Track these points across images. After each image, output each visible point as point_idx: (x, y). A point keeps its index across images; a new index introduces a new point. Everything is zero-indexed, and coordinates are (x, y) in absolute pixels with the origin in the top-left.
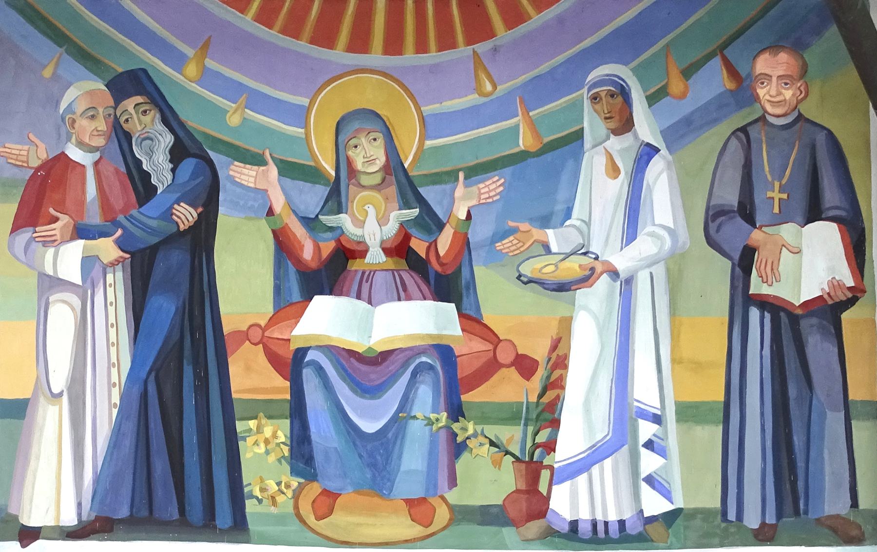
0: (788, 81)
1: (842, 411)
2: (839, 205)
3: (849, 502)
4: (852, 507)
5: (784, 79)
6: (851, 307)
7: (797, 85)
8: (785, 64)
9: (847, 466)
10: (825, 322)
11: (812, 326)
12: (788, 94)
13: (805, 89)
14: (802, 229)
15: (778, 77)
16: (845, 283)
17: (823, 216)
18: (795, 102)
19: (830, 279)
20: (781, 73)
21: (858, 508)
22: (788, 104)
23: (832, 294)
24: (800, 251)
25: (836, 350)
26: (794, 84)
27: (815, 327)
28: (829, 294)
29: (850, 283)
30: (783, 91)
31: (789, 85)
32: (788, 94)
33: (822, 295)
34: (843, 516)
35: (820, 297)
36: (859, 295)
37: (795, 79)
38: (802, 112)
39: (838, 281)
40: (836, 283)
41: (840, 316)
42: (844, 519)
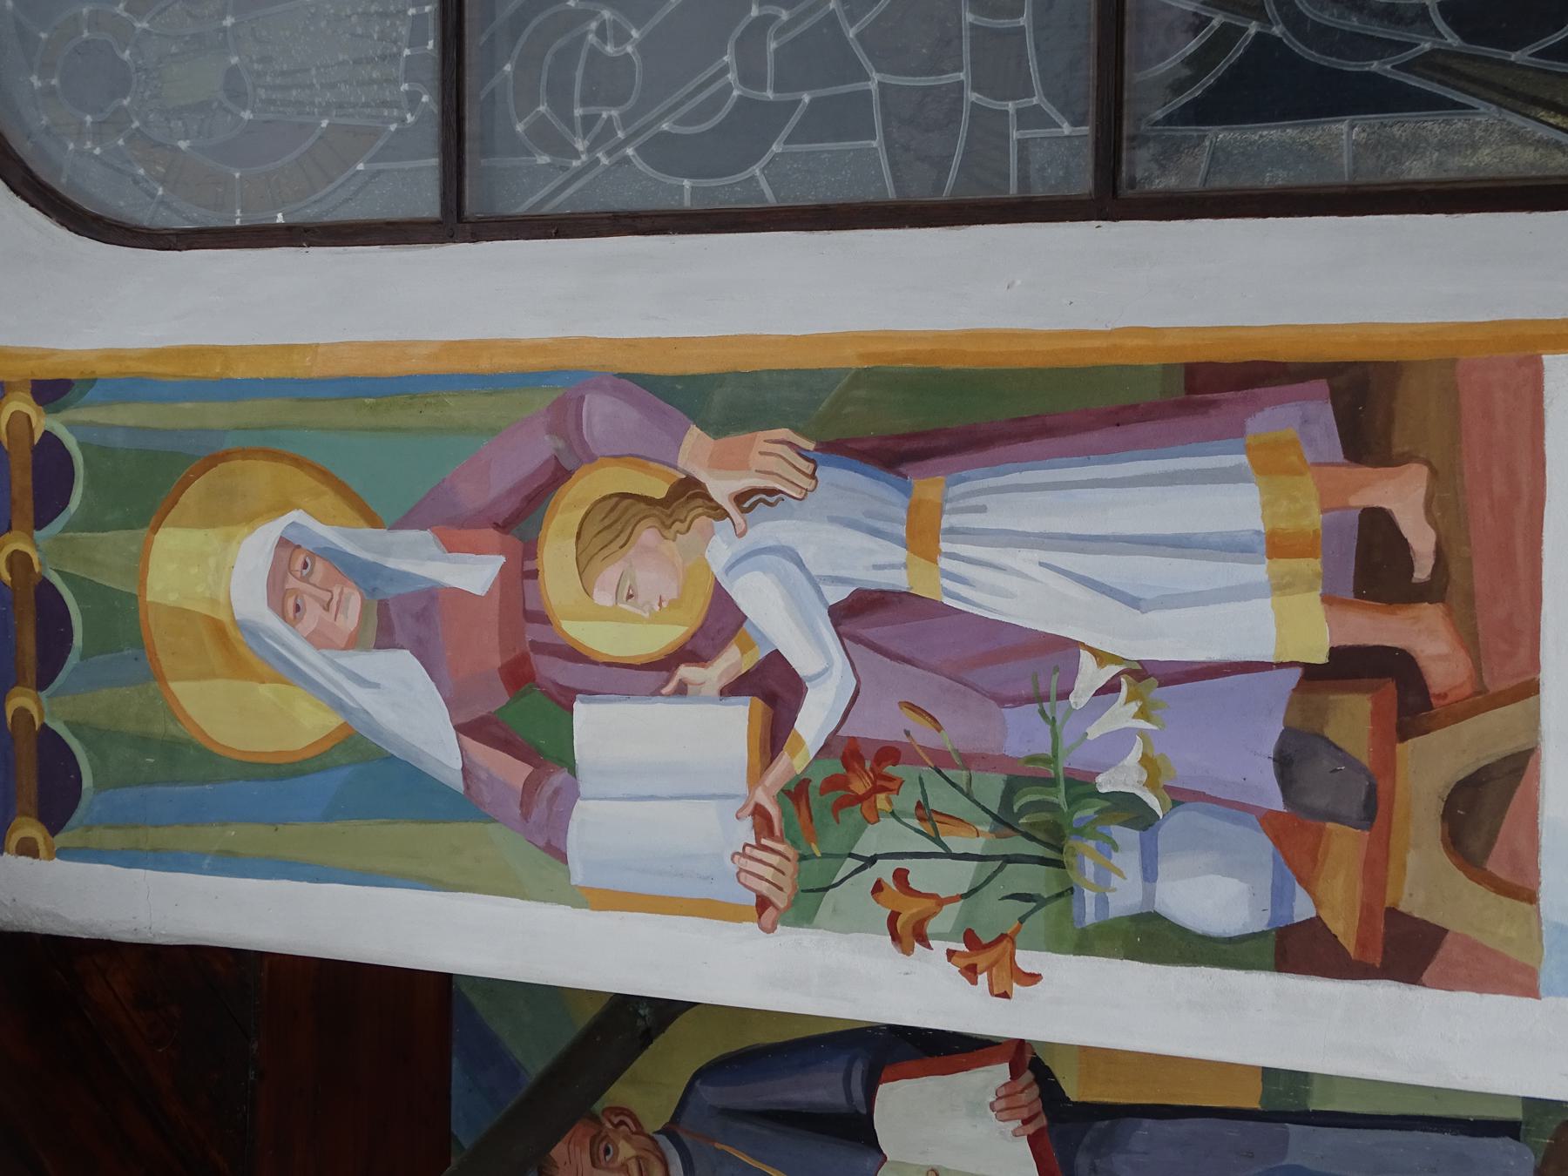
0: (602, 1146)
1: (1286, 1127)
2: (840, 1075)
3: (1504, 1143)
4: (1517, 1138)
5: (598, 1154)
6: (1053, 1076)
7: (609, 1129)
8: (571, 1146)
9: (1417, 1136)
10: (1087, 1140)
11: (1094, 1169)
12: (626, 1151)
13: (617, 1115)
14: (888, 1159)
15: (594, 1165)
16: (1003, 1082)
17: (864, 1111)
18: (643, 1138)
19: (993, 1114)
20: (586, 1157)
21: (1521, 1123)
22: (642, 1154)
23: (1026, 1114)
24: (933, 1170)
25: (1147, 1123)
26: (607, 1136)
27: (1097, 1162)
28: (1025, 1122)
29: (1000, 1073)
30: (620, 1159)
31: (610, 1147)
32: (626, 1151)
33: (1029, 1137)
34: (1539, 1160)
35: (1033, 1141)
36: (1029, 1056)
37: (601, 1132)
38: (659, 1128)
39: (999, 1098)
40: (1002, 1104)
41: (1073, 1103)
42: (1546, 1161)
